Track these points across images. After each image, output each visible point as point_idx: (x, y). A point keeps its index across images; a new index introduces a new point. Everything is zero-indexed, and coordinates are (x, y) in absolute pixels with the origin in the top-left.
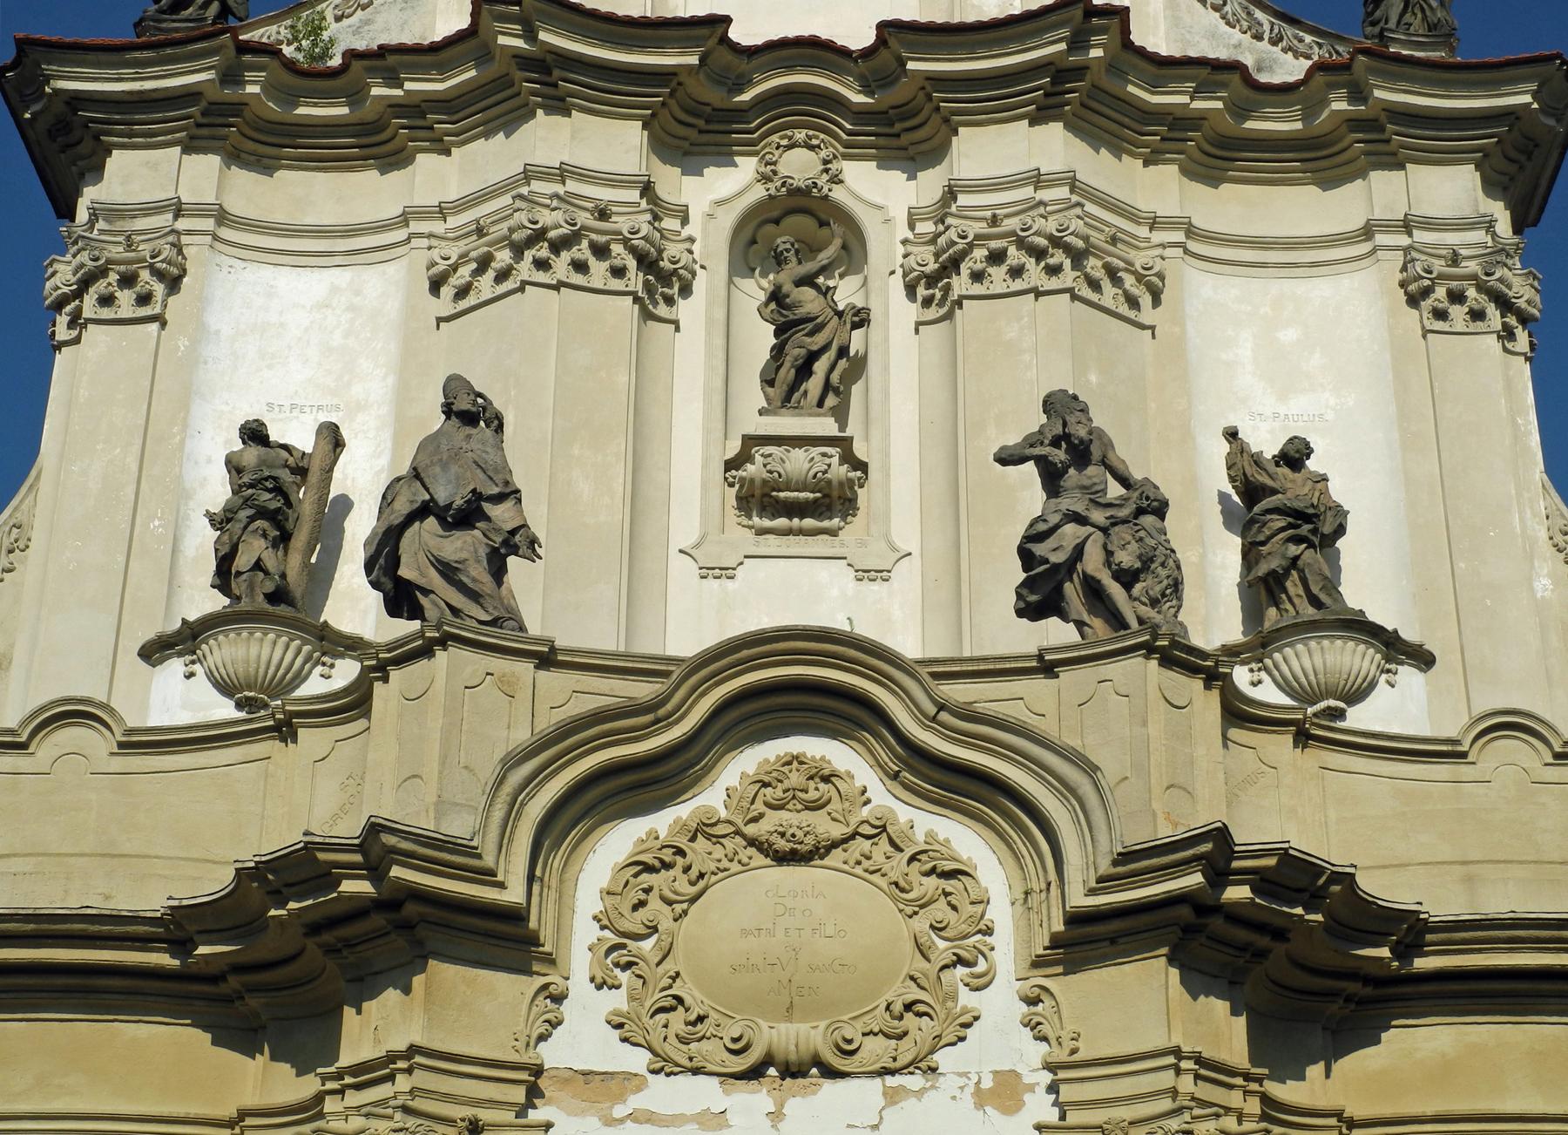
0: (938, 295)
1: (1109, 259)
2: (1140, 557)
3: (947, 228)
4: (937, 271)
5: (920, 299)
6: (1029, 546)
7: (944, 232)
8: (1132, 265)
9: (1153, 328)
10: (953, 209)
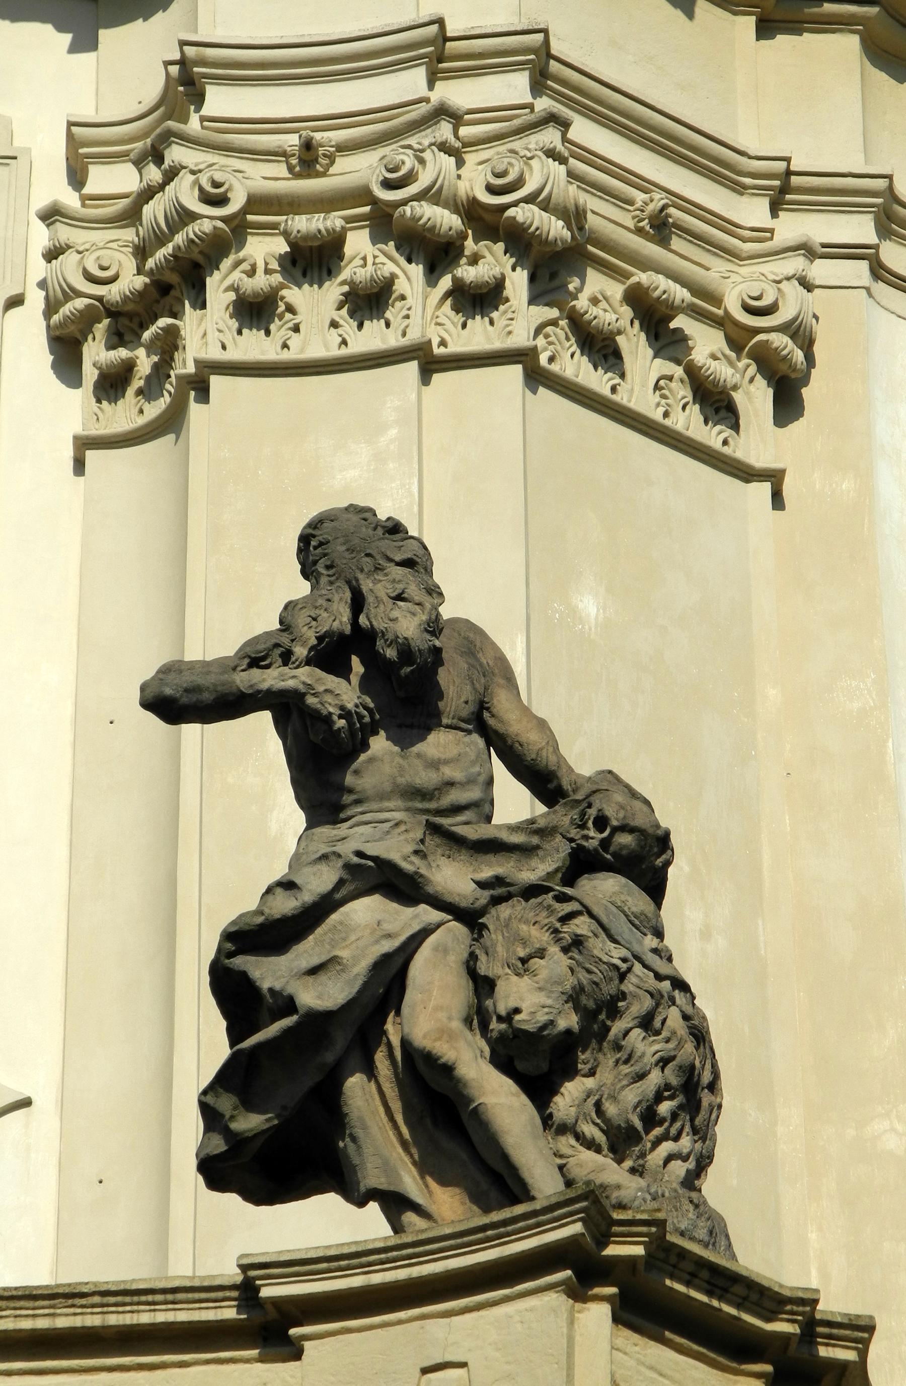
0: (145, 363)
1: (643, 277)
2: (574, 998)
3: (171, 175)
4: (141, 295)
5: (90, 374)
6: (240, 962)
7: (162, 187)
8: (716, 300)
9: (775, 478)
10: (194, 125)
